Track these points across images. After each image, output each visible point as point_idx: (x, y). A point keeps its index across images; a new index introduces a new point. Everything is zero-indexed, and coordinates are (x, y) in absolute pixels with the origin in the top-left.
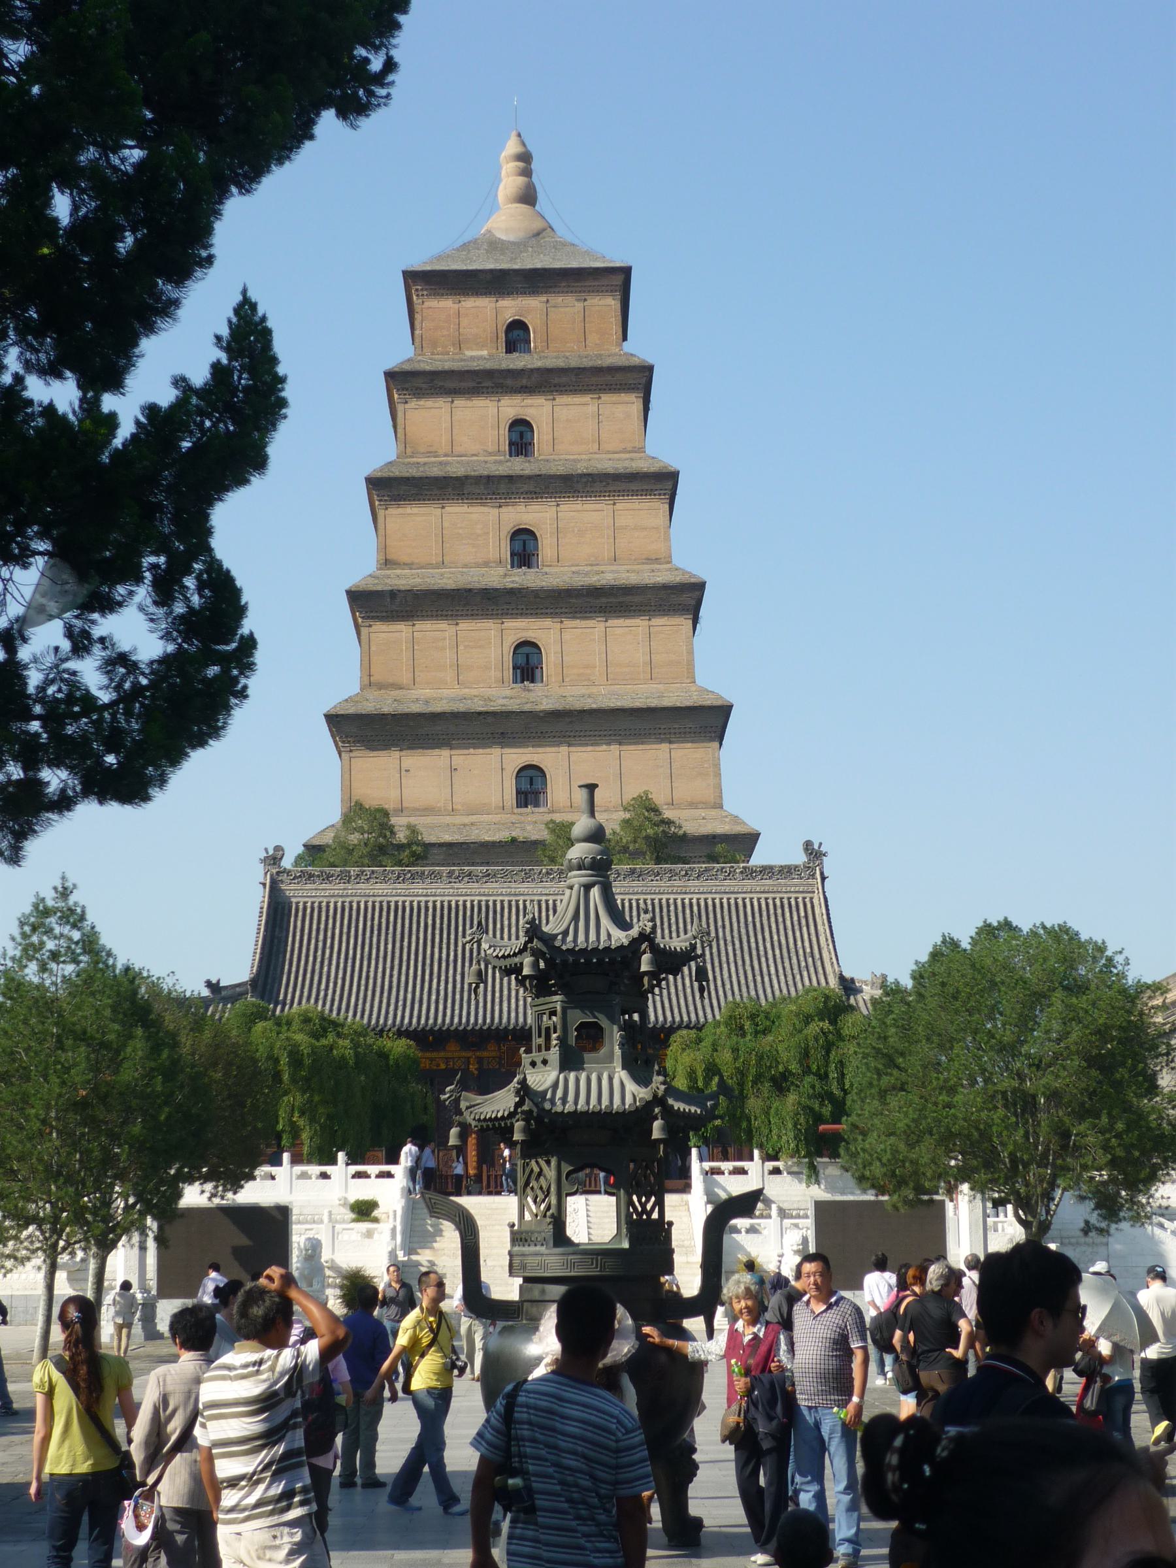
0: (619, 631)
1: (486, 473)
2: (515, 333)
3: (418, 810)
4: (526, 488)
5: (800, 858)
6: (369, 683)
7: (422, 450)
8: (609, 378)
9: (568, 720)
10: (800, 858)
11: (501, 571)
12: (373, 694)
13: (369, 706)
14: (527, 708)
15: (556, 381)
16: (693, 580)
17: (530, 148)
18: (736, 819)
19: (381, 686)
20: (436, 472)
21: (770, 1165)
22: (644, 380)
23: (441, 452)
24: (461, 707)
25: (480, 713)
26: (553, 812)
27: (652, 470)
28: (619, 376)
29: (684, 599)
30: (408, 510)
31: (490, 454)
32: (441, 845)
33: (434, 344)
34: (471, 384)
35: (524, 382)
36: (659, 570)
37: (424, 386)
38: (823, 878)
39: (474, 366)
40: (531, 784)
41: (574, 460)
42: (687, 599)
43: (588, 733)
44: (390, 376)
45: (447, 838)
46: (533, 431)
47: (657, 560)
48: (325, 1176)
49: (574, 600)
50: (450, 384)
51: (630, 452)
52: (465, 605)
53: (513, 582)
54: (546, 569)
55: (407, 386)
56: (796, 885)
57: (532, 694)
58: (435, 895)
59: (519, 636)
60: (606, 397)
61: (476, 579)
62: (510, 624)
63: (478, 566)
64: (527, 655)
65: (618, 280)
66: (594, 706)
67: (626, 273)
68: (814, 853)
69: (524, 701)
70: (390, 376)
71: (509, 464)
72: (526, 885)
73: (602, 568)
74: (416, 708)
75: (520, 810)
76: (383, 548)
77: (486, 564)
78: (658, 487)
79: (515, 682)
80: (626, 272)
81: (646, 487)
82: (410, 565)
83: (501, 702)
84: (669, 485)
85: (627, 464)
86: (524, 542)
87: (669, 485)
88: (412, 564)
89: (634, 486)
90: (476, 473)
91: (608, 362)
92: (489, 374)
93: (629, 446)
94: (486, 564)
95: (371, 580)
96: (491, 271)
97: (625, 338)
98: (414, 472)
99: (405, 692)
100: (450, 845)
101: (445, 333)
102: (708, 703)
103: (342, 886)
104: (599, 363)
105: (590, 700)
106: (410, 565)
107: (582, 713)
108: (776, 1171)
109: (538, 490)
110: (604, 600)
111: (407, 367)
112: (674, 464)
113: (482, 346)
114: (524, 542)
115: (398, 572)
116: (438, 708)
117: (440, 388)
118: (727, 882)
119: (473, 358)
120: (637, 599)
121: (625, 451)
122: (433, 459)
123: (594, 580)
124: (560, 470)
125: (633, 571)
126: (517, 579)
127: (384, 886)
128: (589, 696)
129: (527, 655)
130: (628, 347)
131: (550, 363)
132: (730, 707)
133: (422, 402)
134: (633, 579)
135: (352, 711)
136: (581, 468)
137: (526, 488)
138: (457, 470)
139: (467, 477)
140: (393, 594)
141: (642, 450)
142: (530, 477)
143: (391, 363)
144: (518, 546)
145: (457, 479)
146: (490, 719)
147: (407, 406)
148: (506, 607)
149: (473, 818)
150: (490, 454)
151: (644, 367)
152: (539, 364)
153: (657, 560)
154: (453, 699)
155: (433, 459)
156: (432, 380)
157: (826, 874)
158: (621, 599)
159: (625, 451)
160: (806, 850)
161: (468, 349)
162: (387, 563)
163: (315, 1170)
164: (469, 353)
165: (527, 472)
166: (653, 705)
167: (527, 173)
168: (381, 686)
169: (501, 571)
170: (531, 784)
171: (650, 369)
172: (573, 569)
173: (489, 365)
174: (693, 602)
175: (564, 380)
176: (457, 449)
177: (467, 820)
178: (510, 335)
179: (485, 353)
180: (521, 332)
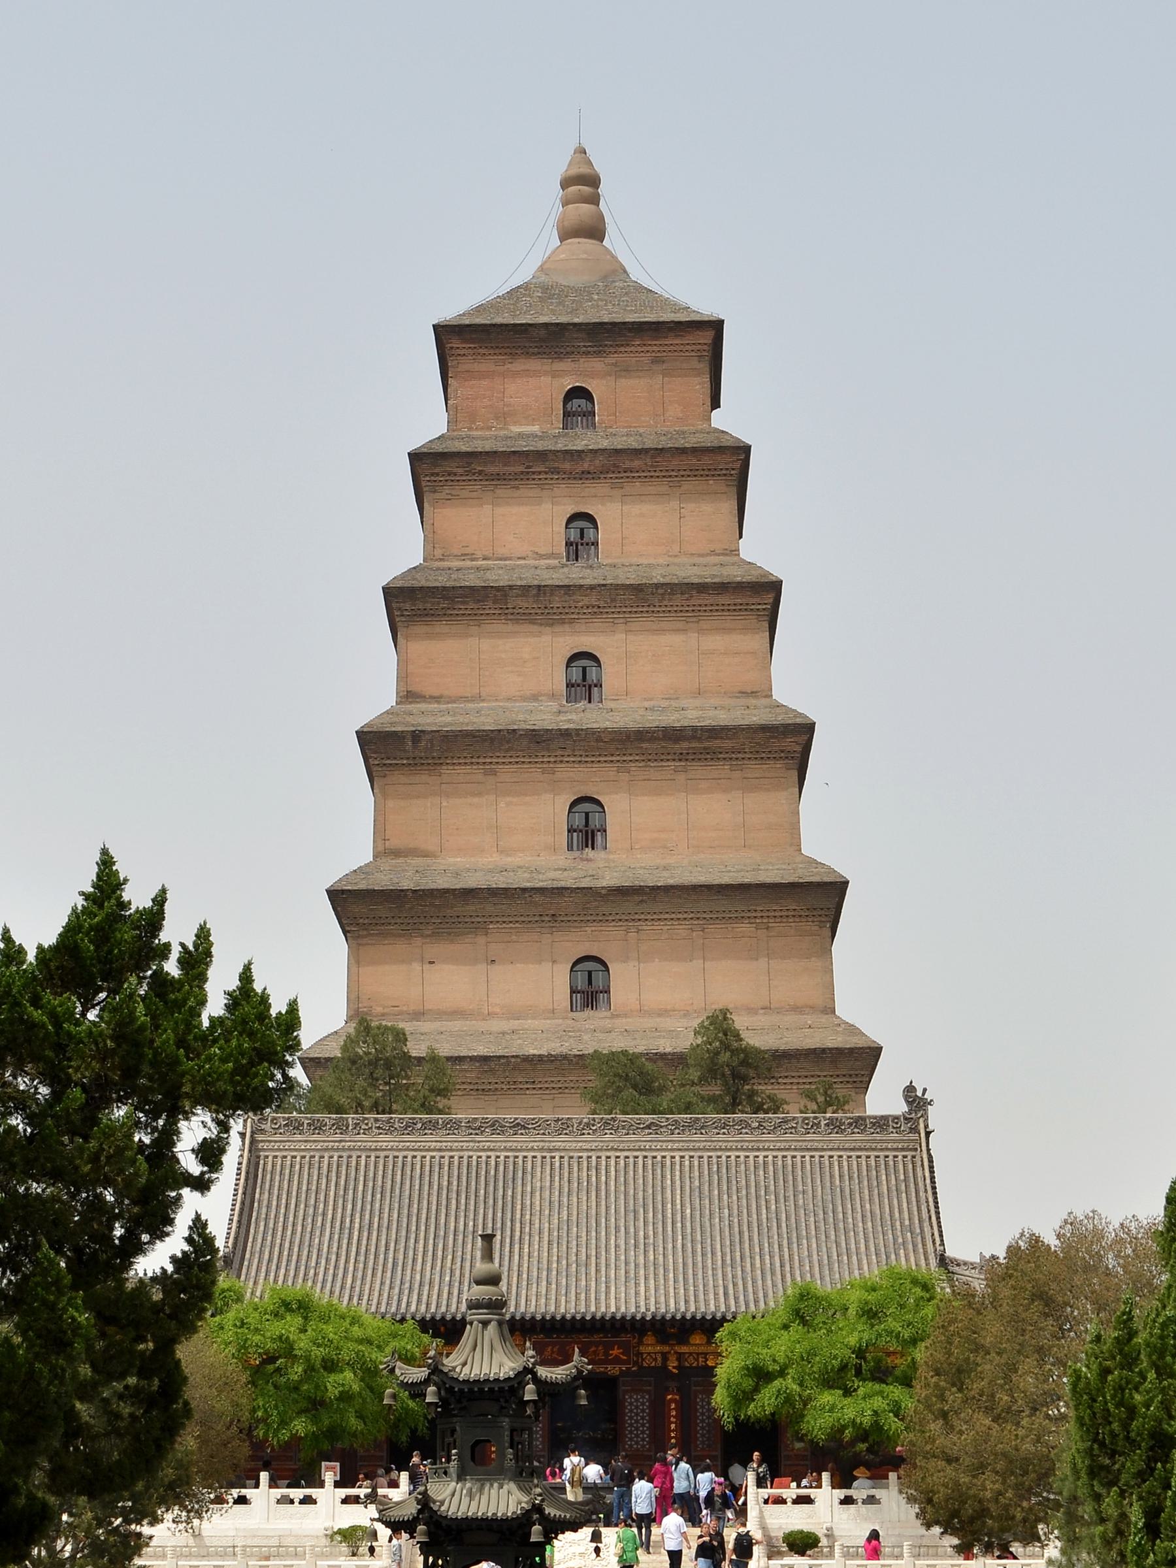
1: (536, 583)
2: (577, 403)
3: (445, 1013)
4: (586, 601)
5: (899, 1107)
6: (384, 850)
7: (456, 552)
8: (694, 461)
9: (637, 898)
10: (899, 1107)
11: (554, 705)
12: (387, 863)
13: (383, 881)
14: (585, 883)
15: (628, 464)
16: (798, 720)
17: (600, 167)
18: (853, 1030)
19: (396, 853)
20: (472, 580)
21: (841, 1493)
22: (738, 465)
23: (479, 554)
24: (499, 881)
25: (524, 890)
26: (618, 1016)
27: (747, 579)
28: (707, 460)
29: (786, 746)
31: (542, 557)
32: (472, 1059)
33: (472, 417)
34: (522, 468)
35: (586, 466)
36: (756, 707)
37: (460, 470)
38: (928, 1134)
39: (523, 446)
40: (590, 982)
41: (649, 566)
42: (792, 744)
43: (662, 916)
44: (416, 458)
45: (481, 1050)
46: (597, 528)
47: (754, 694)
48: (308, 1500)
51: (719, 555)
52: (507, 751)
53: (569, 721)
54: (612, 705)
55: (436, 471)
56: (894, 1141)
57: (592, 865)
58: (451, 1150)
61: (521, 717)
62: (564, 772)
63: (524, 699)
64: (587, 814)
65: (707, 337)
66: (671, 882)
67: (716, 327)
68: (916, 1102)
69: (582, 874)
70: (416, 458)
71: (566, 570)
72: (563, 1137)
73: (684, 703)
74: (443, 883)
75: (574, 1014)
76: (403, 676)
77: (535, 698)
78: (754, 601)
79: (570, 848)
80: (716, 327)
81: (739, 601)
82: (437, 699)
83: (552, 875)
84: (769, 598)
85: (715, 571)
86: (584, 669)
87: (769, 598)
88: (441, 697)
89: (725, 599)
90: (523, 583)
91: (690, 442)
92: (542, 455)
93: (718, 547)
94: (535, 698)
95: (387, 719)
96: (546, 325)
97: (715, 403)
98: (441, 581)
99: (429, 861)
100: (485, 1059)
101: (486, 402)
102: (816, 879)
103: (338, 1137)
104: (681, 443)
105: (666, 874)
106: (437, 699)
107: (655, 889)
108: (847, 1501)
110: (685, 745)
111: (439, 448)
112: (776, 570)
113: (533, 422)
114: (584, 669)
115: (423, 706)
116: (471, 882)
117: (480, 472)
118: (810, 1137)
119: (521, 435)
120: (728, 744)
121: (713, 553)
122: (468, 563)
123: (672, 719)
124: (632, 579)
125: (723, 708)
126: (573, 717)
127: (388, 1138)
128: (665, 868)
129: (587, 814)
130: (719, 419)
131: (619, 443)
132: (845, 884)
134: (722, 718)
135: (362, 886)
136: (658, 577)
137: (586, 601)
138: (498, 577)
139: (511, 587)
140: (416, 736)
141: (735, 552)
142: (592, 588)
143: (417, 442)
144: (576, 675)
145: (498, 589)
146: (537, 898)
147: (437, 496)
148: (560, 752)
149: (515, 1024)
150: (542, 557)
151: (739, 448)
152: (605, 444)
153: (754, 694)
154: (490, 871)
155: (468, 563)
156: (470, 464)
157: (931, 1128)
158: (707, 744)
159: (713, 553)
160: (906, 1098)
161: (515, 423)
162: (407, 695)
163: (297, 1493)
164: (516, 429)
165: (588, 582)
166: (746, 881)
167: (595, 200)
168: (396, 853)
169: (554, 705)
170: (590, 982)
171: (746, 450)
172: (647, 704)
173: (541, 446)
174: (799, 749)
175: (637, 463)
176: (501, 551)
177: (506, 1025)
178: (569, 406)
179: (535, 428)
180: (583, 402)
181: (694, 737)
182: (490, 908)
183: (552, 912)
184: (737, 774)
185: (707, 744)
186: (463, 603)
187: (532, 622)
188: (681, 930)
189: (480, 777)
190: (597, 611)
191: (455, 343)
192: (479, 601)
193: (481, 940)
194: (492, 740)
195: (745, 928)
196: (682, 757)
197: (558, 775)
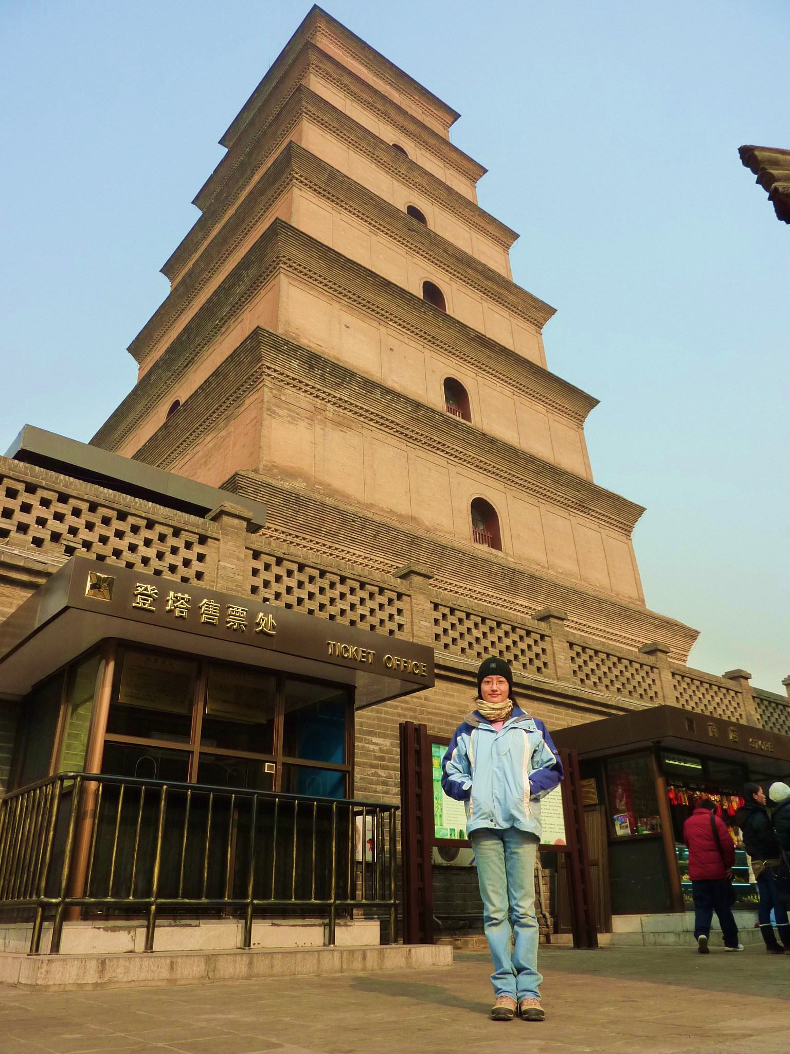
0: (497, 316)
9: (487, 352)
28: (465, 163)
30: (328, 136)
34: (371, 100)
37: (335, 76)
49: (470, 271)
50: (352, 87)
52: (388, 223)
55: (321, 65)
59: (427, 275)
60: (452, 171)
89: (490, 228)
109: (428, 188)
110: (490, 284)
120: (512, 298)
133: (330, 86)
156: (342, 76)
181: (497, 283)
182: (393, 308)
183: (433, 334)
184: (512, 320)
185: (502, 291)
186: (348, 131)
187: (387, 173)
188: (507, 391)
189: (367, 232)
190: (424, 192)
191: (322, 25)
192: (358, 138)
193: (382, 329)
194: (382, 209)
195: (540, 408)
196: (485, 292)
197: (415, 260)
